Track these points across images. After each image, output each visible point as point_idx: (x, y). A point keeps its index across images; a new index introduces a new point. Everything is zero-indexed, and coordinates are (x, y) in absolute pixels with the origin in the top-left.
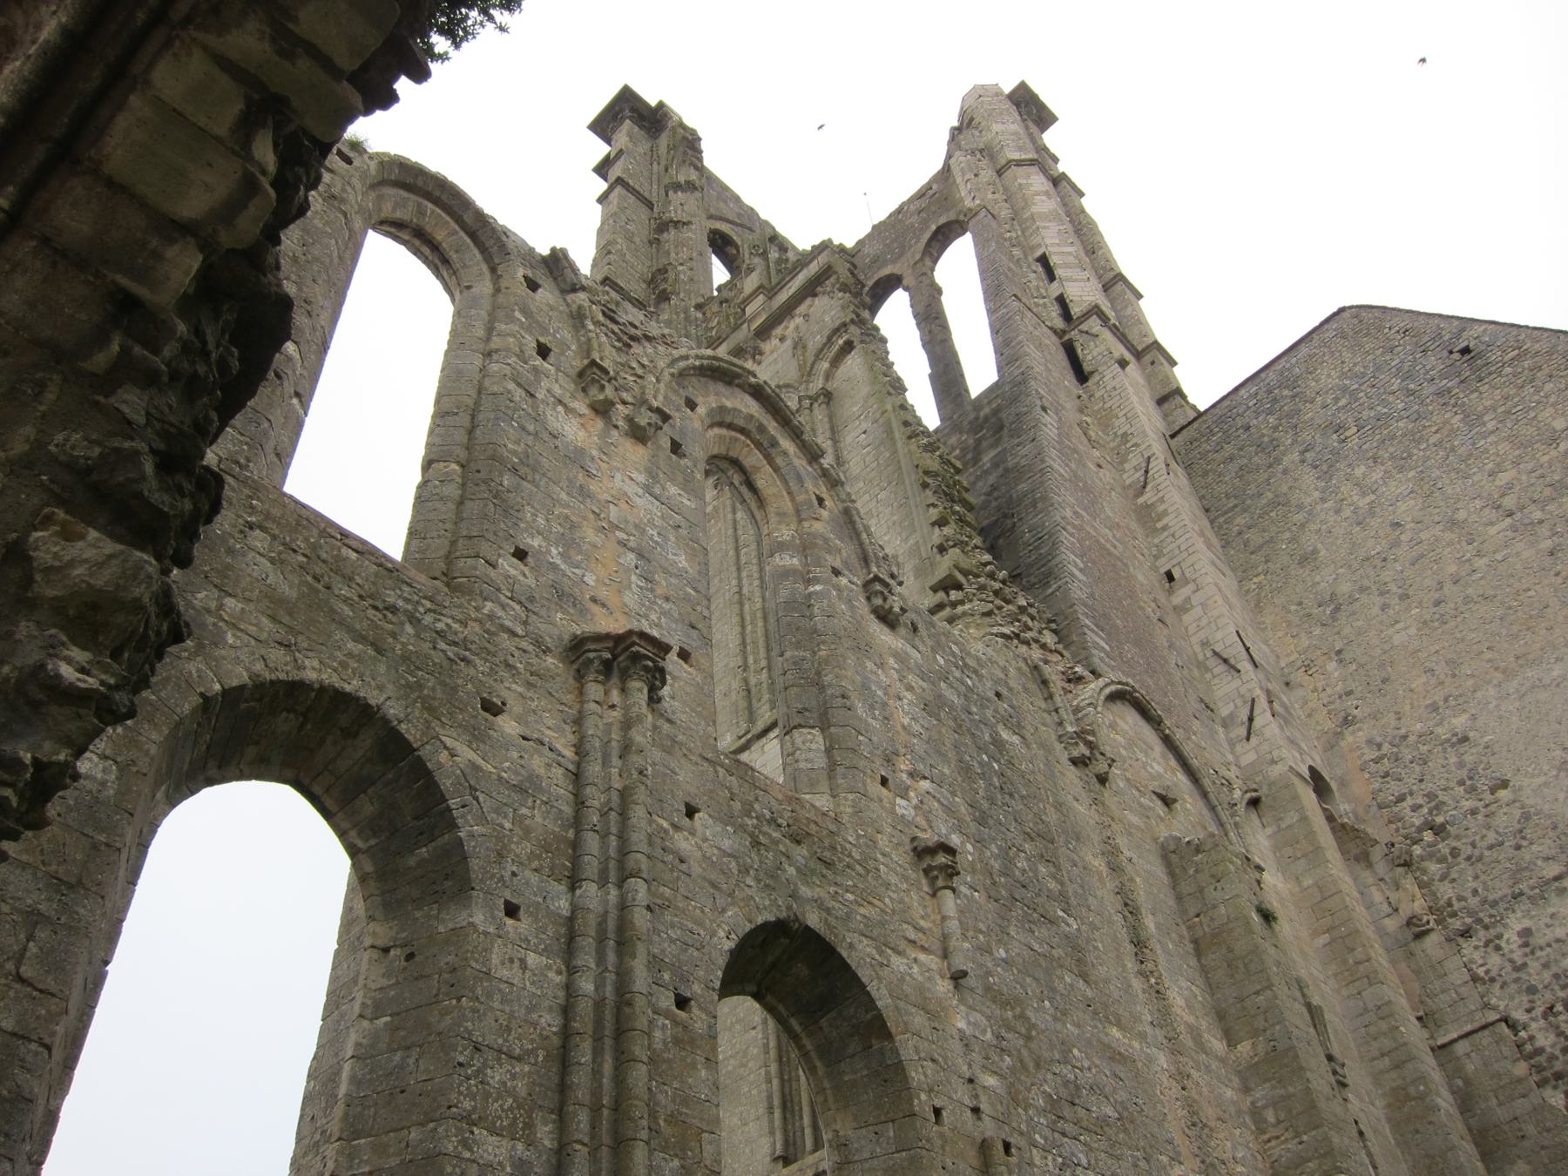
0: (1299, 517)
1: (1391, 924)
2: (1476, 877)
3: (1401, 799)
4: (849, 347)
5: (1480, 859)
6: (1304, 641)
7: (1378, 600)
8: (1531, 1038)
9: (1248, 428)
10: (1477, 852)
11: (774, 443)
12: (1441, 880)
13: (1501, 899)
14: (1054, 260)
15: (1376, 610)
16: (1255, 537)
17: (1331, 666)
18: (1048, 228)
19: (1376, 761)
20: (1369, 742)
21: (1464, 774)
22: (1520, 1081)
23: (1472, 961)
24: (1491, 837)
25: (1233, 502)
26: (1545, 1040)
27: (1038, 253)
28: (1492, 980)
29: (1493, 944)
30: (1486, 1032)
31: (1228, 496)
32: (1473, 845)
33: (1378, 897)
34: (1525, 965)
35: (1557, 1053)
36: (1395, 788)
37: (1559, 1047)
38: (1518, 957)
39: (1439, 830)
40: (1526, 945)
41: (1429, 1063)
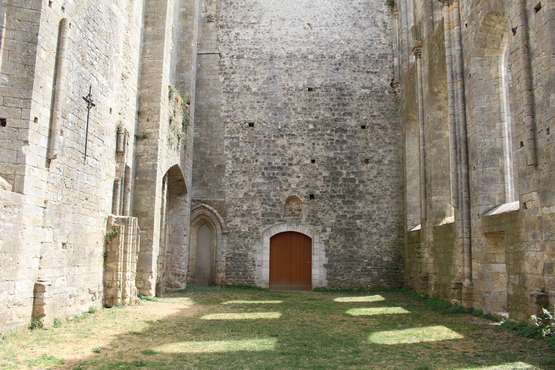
1: (203, 15)
2: (233, 13)
5: (237, 9)
8: (224, 61)
10: (237, 6)
12: (223, 9)
13: (237, 22)
22: (215, 71)
23: (219, 35)
24: (244, 4)
26: (227, 63)
28: (222, 42)
29: (227, 33)
30: (213, 55)
32: (237, 4)
33: (203, 6)
34: (233, 42)
35: (228, 68)
37: (230, 66)
38: (232, 40)
40: (236, 37)
41: (195, 56)
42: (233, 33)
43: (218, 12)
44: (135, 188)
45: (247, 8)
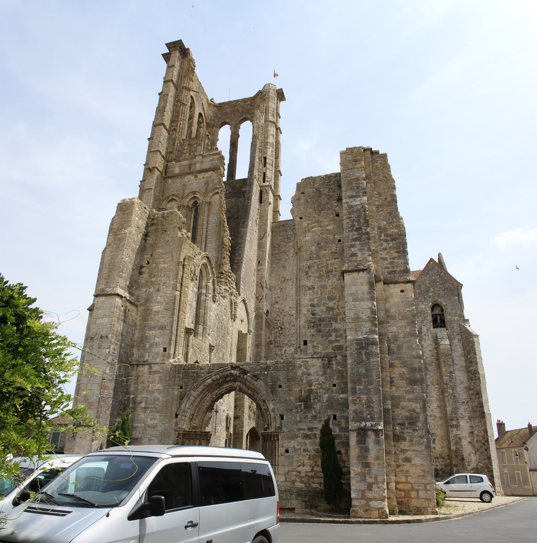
0: (287, 257)
1: (268, 340)
3: (279, 320)
4: (217, 193)
6: (276, 284)
7: (292, 283)
9: (287, 231)
11: (207, 267)
14: (268, 161)
15: (290, 285)
16: (278, 257)
17: (279, 291)
18: (269, 148)
19: (278, 312)
20: (279, 308)
21: (289, 321)
24: (288, 333)
25: (277, 246)
27: (265, 156)
29: (280, 350)
31: (277, 244)
36: (278, 318)
39: (282, 328)
42: (283, 350)
43: (275, 338)
44: (234, 441)
45: (290, 336)
